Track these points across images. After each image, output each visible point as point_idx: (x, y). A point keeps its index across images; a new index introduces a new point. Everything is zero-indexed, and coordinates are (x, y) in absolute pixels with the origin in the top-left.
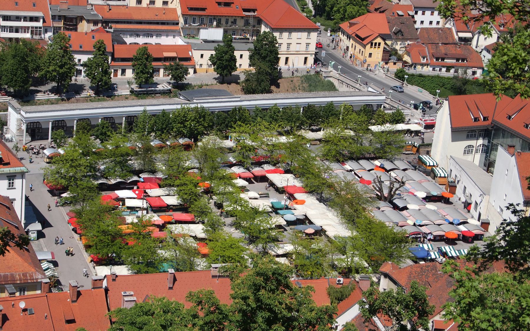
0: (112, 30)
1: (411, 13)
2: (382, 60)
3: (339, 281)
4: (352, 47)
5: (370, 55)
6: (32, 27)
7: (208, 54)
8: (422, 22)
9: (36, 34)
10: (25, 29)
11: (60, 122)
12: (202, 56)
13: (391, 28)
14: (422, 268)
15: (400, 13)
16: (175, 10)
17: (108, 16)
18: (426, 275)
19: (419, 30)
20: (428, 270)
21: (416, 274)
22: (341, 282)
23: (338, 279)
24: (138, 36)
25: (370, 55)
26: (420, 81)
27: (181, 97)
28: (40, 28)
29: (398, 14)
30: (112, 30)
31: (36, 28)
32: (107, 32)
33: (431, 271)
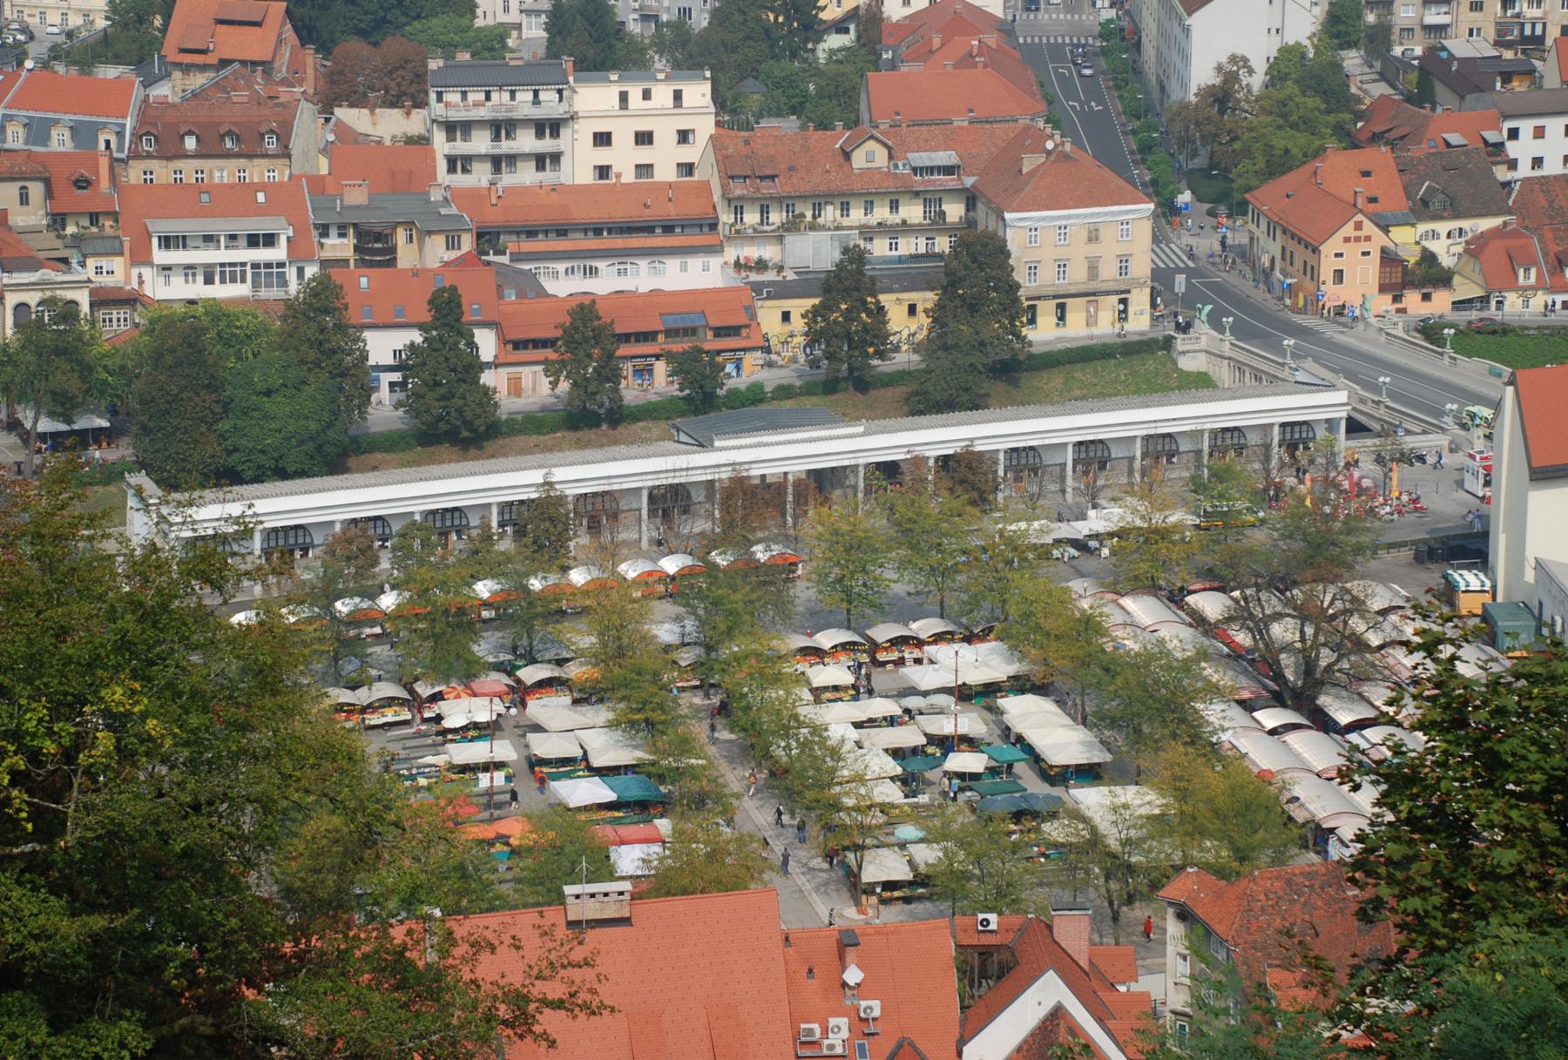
0: (505, 259)
1: (1492, 136)
2: (1383, 289)
3: (986, 922)
4: (1283, 258)
5: (1339, 276)
6: (255, 266)
7: (799, 307)
8: (1537, 162)
9: (269, 285)
10: (231, 273)
11: (292, 533)
12: (786, 317)
13: (1409, 192)
14: (1289, 882)
15: (1455, 138)
16: (706, 186)
17: (493, 218)
18: (1305, 905)
19: (1517, 187)
20: (1311, 887)
21: (1268, 898)
22: (993, 926)
23: (981, 916)
24: (592, 272)
25: (1339, 276)
26: (1488, 338)
27: (683, 438)
28: (281, 265)
29: (1448, 145)
30: (505, 259)
31: (269, 265)
32: (489, 263)
33: (1322, 888)
